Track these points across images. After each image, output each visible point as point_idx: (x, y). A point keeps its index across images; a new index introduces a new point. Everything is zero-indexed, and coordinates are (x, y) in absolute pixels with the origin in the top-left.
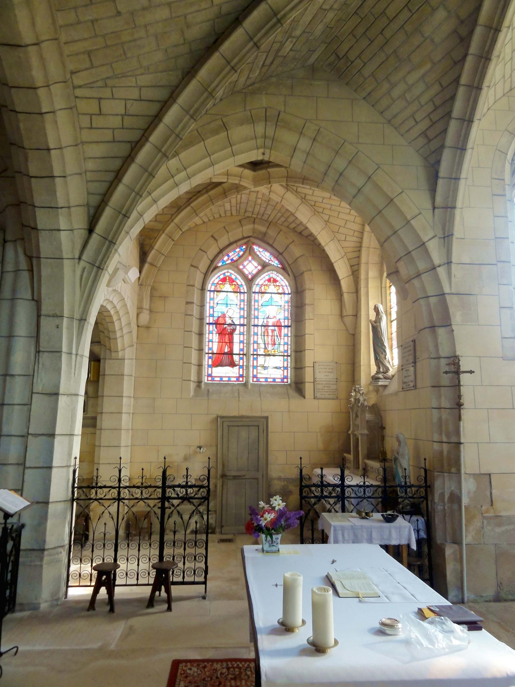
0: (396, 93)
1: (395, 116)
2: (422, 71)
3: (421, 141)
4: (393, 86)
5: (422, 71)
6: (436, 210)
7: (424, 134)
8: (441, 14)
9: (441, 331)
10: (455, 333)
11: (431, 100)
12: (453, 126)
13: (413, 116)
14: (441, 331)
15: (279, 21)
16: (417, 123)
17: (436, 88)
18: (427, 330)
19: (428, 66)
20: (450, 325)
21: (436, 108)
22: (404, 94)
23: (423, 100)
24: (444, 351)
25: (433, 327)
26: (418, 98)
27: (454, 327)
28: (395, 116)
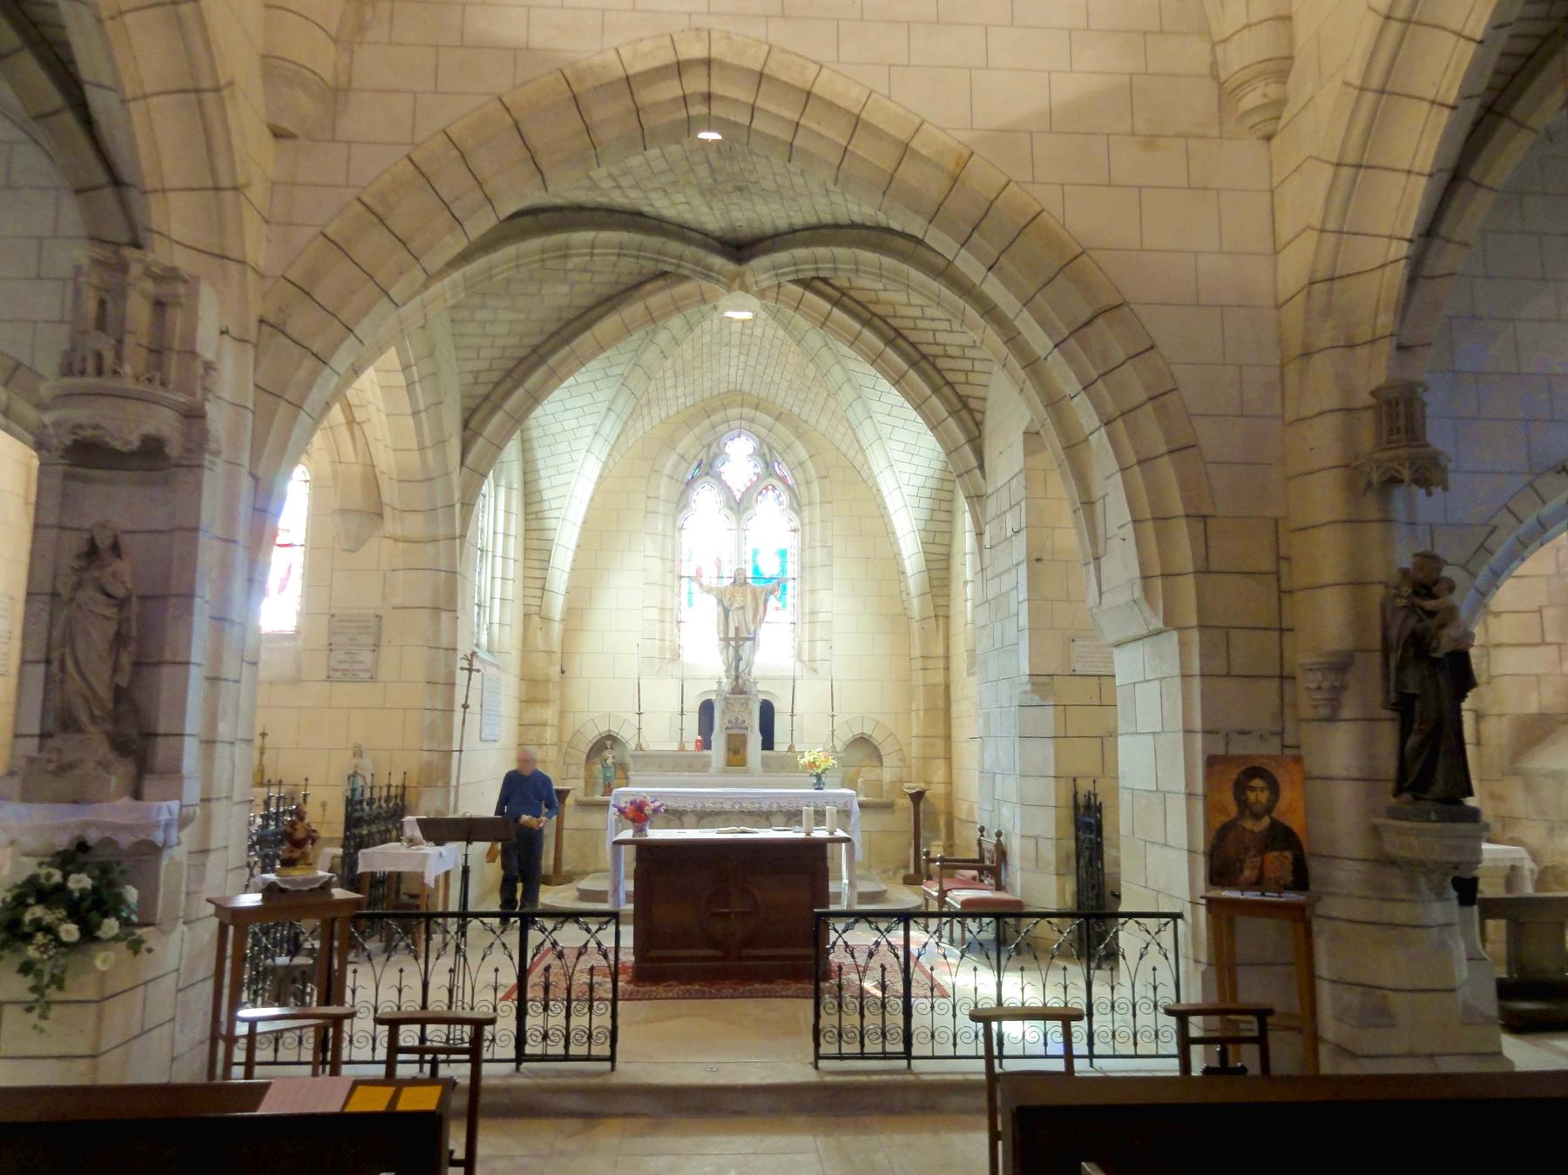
0: (480, 315)
1: (463, 335)
2: (513, 316)
3: (469, 378)
4: (483, 306)
5: (513, 316)
6: (464, 469)
7: (477, 373)
8: (564, 289)
9: (444, 615)
10: (459, 621)
11: (504, 348)
12: (519, 394)
13: (479, 349)
14: (444, 615)
15: (566, 256)
16: (478, 358)
17: (512, 341)
18: (428, 611)
19: (521, 316)
20: (455, 611)
21: (501, 358)
22: (486, 323)
23: (499, 342)
24: (444, 643)
25: (436, 609)
26: (495, 336)
27: (459, 614)
28: (463, 335)
